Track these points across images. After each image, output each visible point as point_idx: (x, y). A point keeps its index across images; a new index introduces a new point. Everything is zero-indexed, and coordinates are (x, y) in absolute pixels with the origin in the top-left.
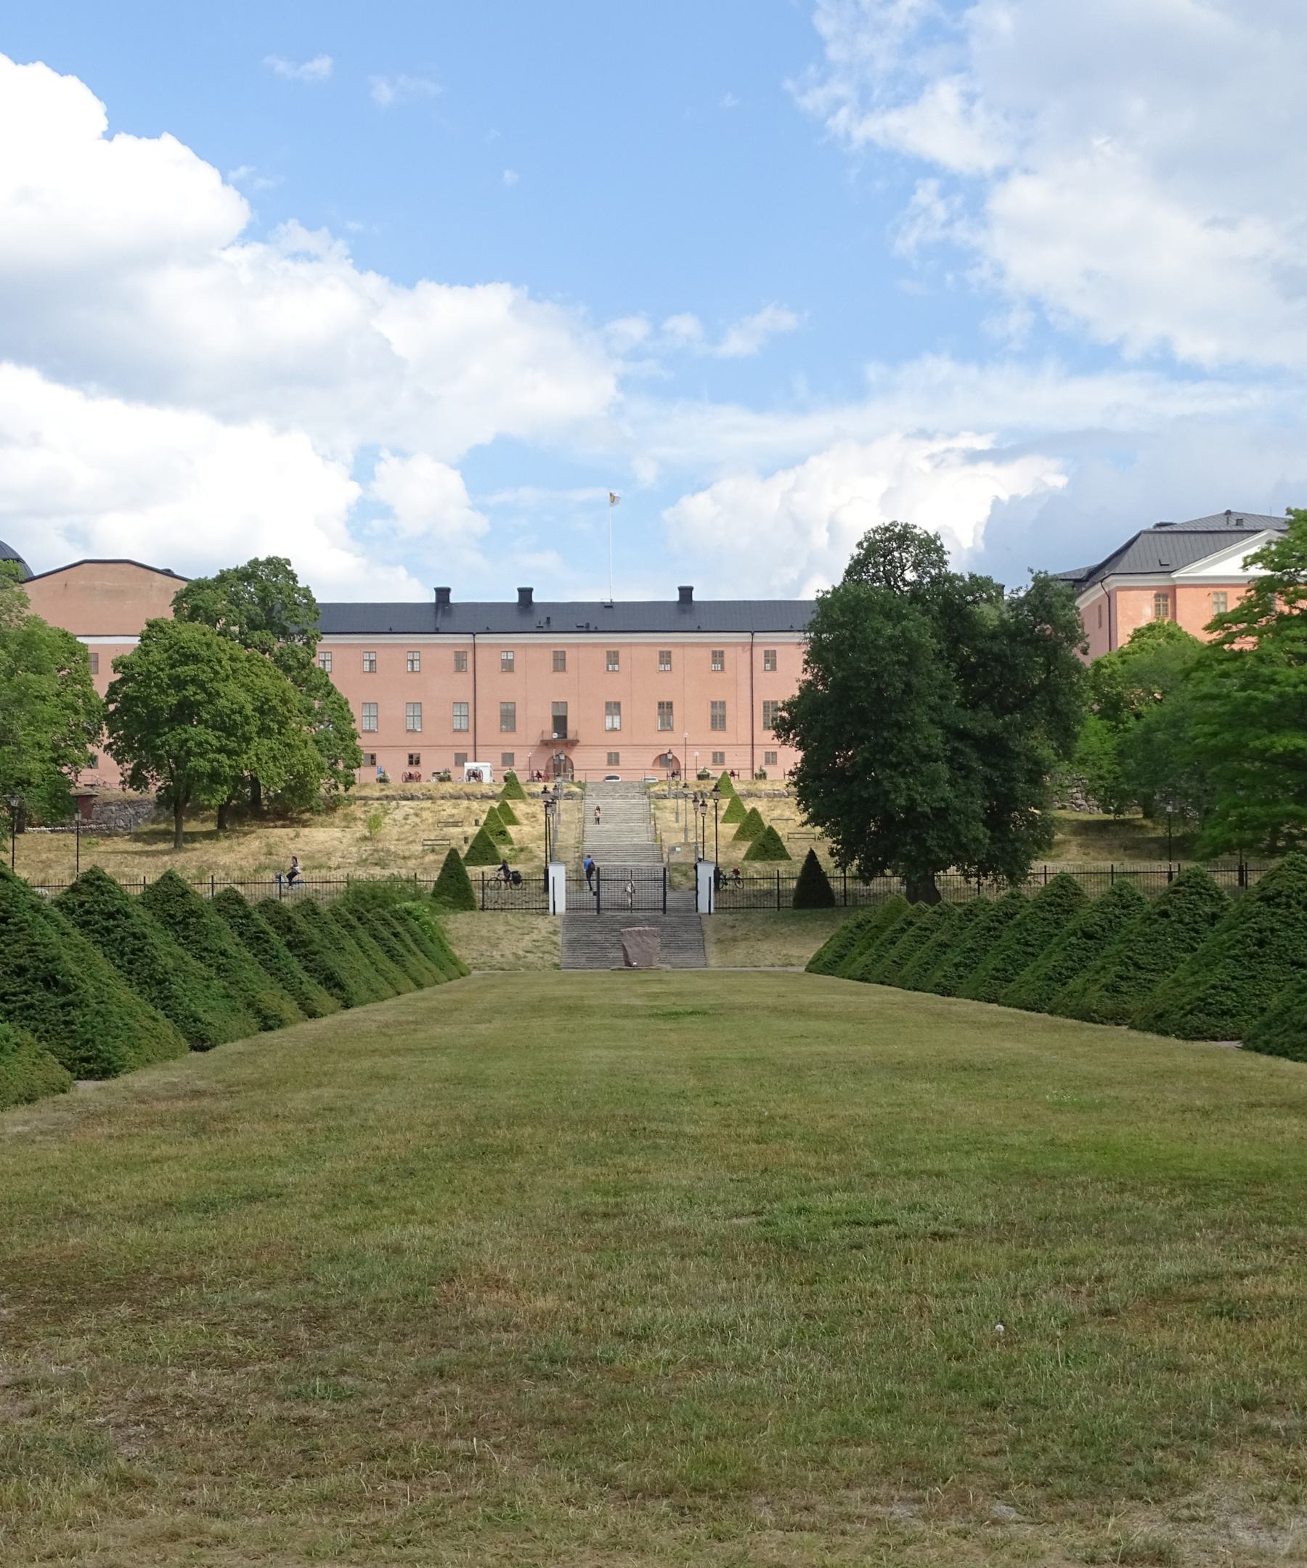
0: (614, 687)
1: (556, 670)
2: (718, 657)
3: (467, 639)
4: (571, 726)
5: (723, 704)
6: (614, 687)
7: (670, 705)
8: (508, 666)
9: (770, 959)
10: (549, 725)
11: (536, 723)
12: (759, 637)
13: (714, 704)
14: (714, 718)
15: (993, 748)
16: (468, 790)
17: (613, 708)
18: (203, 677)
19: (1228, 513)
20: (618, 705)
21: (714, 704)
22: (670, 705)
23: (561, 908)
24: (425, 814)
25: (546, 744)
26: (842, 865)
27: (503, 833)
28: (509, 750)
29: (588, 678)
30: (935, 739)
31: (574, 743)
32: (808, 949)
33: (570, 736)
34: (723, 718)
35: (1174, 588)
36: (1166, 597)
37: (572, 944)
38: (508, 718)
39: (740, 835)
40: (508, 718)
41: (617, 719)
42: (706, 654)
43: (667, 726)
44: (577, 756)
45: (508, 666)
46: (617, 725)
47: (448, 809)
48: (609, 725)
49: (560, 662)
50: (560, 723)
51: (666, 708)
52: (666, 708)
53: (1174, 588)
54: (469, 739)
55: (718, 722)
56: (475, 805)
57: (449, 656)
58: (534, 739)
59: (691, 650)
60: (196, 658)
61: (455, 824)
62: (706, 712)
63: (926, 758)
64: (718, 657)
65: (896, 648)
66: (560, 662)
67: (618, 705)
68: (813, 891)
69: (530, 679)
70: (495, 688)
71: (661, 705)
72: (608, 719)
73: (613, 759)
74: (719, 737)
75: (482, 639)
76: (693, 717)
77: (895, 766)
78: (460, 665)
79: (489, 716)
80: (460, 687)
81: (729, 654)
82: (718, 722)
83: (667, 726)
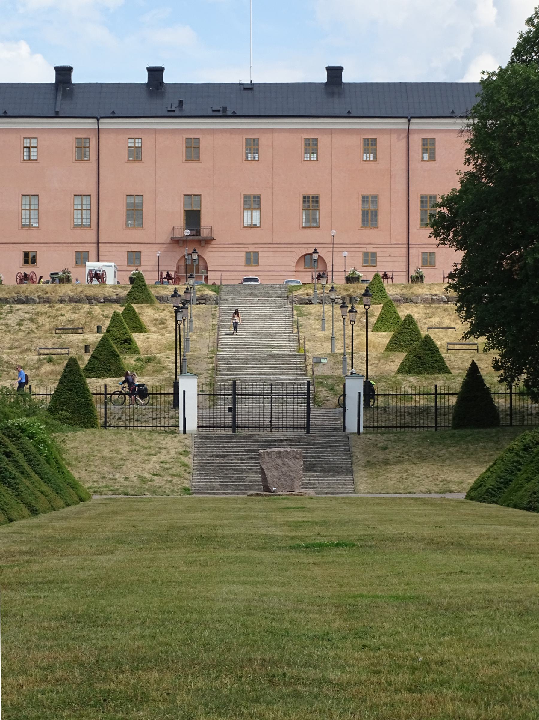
2: (370, 145)
3: (90, 124)
4: (206, 221)
5: (375, 198)
7: (316, 199)
8: (135, 155)
9: (427, 484)
10: (180, 221)
11: (165, 218)
12: (416, 124)
13: (365, 198)
14: (365, 213)
16: (89, 292)
17: (253, 201)
20: (257, 198)
21: (365, 198)
22: (316, 199)
23: (192, 425)
24: (41, 320)
25: (177, 242)
26: (508, 379)
27: (129, 341)
28: (135, 248)
29: (221, 168)
31: (207, 241)
32: (465, 475)
33: (204, 233)
34: (375, 213)
37: (204, 466)
38: (135, 212)
39: (394, 346)
40: (135, 212)
42: (357, 142)
43: (312, 223)
44: (212, 256)
45: (135, 155)
46: (256, 221)
47: (68, 314)
48: (247, 221)
49: (193, 151)
50: (193, 217)
51: (311, 202)
52: (311, 202)
54: (90, 235)
55: (370, 217)
56: (97, 310)
57: (69, 143)
58: (165, 237)
59: (340, 136)
61: (75, 331)
62: (355, 208)
64: (370, 145)
66: (193, 151)
67: (257, 198)
68: (474, 407)
69: (160, 169)
70: (121, 179)
71: (306, 198)
72: (247, 215)
73: (252, 259)
74: (370, 235)
75: (106, 124)
78: (81, 152)
79: (114, 211)
80: (82, 177)
81: (383, 142)
82: (370, 217)
83: (312, 223)
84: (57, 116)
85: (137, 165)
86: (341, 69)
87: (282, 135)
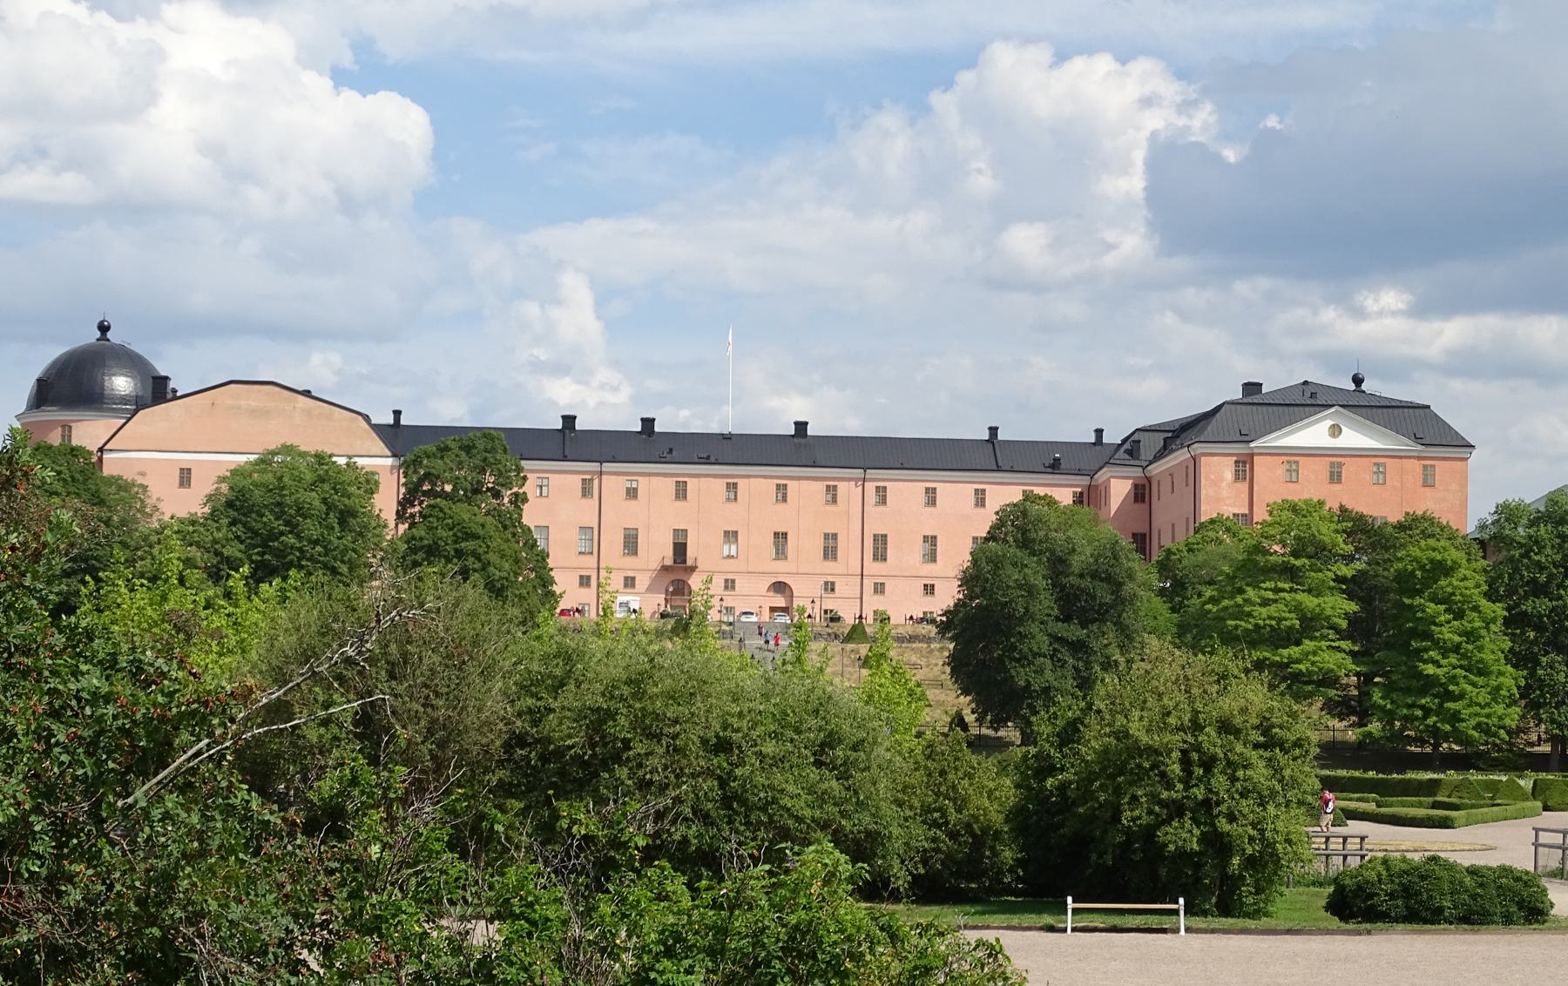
0: (732, 516)
1: (677, 497)
2: (832, 490)
3: (595, 466)
5: (835, 536)
6: (732, 516)
7: (785, 535)
8: (632, 493)
10: (669, 553)
11: (657, 550)
13: (826, 536)
15: (1078, 647)
17: (731, 536)
18: (480, 551)
19: (1306, 383)
21: (826, 536)
22: (785, 535)
25: (665, 569)
28: (631, 574)
29: (705, 507)
30: (1042, 642)
31: (693, 569)
33: (689, 562)
34: (835, 549)
35: (1252, 455)
36: (1244, 467)
38: (631, 543)
40: (631, 543)
41: (733, 548)
42: (821, 486)
44: (695, 582)
46: (733, 553)
48: (726, 553)
49: (681, 492)
50: (680, 549)
51: (781, 538)
52: (781, 538)
53: (1252, 455)
54: (591, 561)
55: (830, 552)
57: (576, 480)
60: (476, 537)
62: (819, 544)
63: (1036, 655)
64: (832, 490)
65: (1020, 587)
66: (681, 492)
69: (652, 505)
70: (619, 516)
72: (726, 547)
74: (830, 566)
75: (607, 467)
76: (806, 546)
77: (1018, 660)
78: (586, 491)
79: (612, 542)
80: (585, 512)
81: (842, 487)
82: (830, 552)
84: (565, 459)
85: (634, 502)
86: (806, 423)
87: (757, 485)
